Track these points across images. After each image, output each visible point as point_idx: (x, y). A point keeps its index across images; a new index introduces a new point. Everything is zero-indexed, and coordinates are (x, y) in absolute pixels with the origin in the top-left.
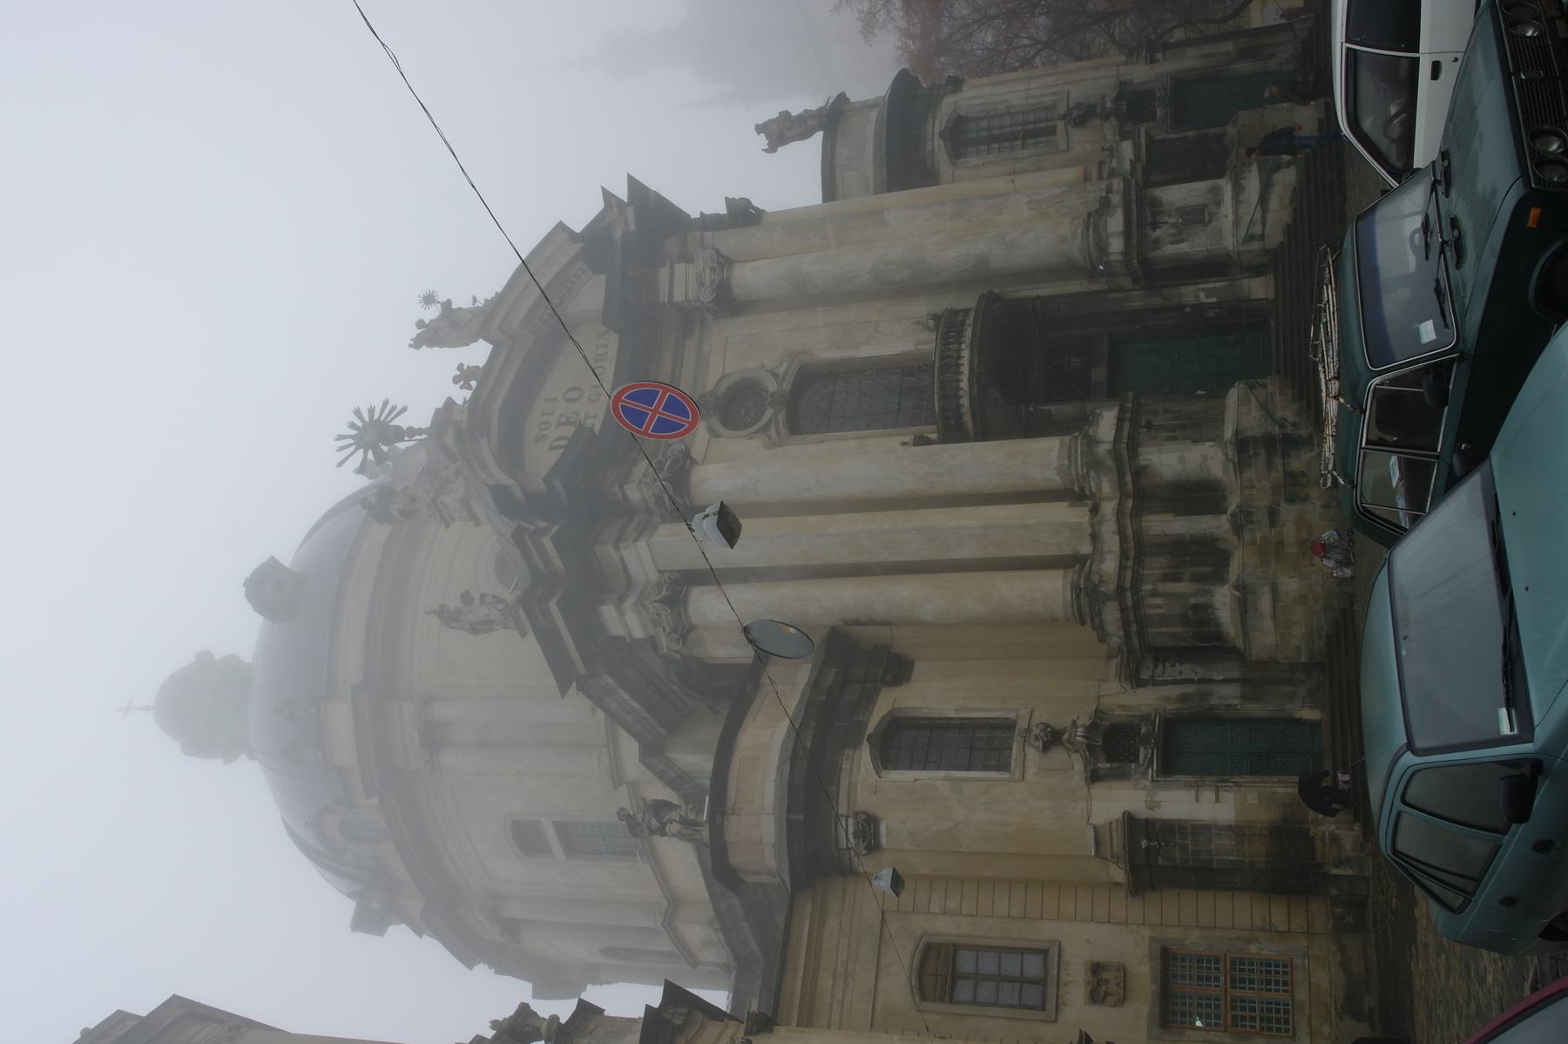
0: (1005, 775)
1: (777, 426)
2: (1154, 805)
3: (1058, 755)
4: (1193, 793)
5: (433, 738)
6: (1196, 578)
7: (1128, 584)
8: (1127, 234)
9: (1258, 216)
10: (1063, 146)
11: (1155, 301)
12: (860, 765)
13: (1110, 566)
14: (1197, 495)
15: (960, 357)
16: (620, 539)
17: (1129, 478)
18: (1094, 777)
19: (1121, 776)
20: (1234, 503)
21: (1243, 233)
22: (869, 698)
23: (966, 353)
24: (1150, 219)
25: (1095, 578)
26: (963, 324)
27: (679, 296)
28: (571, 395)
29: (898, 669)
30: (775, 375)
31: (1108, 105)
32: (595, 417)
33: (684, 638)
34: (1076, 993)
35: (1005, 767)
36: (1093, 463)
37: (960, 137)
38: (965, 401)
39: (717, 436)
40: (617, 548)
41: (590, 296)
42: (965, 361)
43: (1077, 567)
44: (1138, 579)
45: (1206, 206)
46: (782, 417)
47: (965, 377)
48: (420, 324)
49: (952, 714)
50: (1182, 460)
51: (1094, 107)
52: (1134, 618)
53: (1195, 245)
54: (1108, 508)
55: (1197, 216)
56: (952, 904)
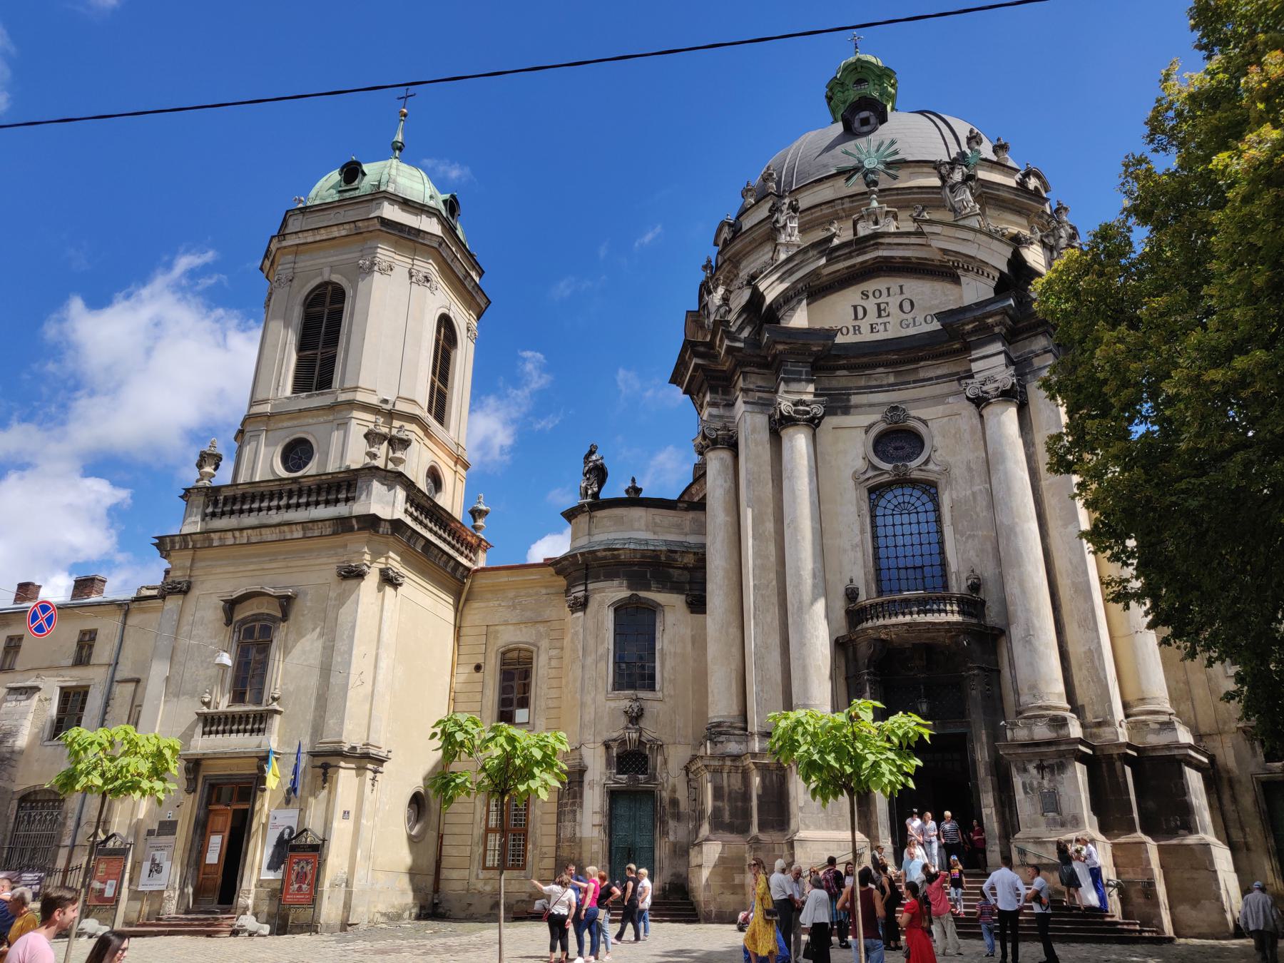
0: (610, 688)
3: (623, 721)
6: (717, 811)
11: (982, 771)
12: (616, 591)
13: (733, 747)
15: (904, 614)
18: (607, 746)
19: (609, 764)
23: (908, 618)
24: (1045, 764)
25: (722, 738)
27: (975, 367)
28: (907, 306)
30: (927, 462)
32: (886, 330)
39: (866, 432)
40: (742, 390)
41: (975, 290)
42: (901, 619)
43: (741, 725)
45: (1060, 814)
46: (885, 478)
49: (658, 646)
53: (1025, 806)
56: (554, 663)
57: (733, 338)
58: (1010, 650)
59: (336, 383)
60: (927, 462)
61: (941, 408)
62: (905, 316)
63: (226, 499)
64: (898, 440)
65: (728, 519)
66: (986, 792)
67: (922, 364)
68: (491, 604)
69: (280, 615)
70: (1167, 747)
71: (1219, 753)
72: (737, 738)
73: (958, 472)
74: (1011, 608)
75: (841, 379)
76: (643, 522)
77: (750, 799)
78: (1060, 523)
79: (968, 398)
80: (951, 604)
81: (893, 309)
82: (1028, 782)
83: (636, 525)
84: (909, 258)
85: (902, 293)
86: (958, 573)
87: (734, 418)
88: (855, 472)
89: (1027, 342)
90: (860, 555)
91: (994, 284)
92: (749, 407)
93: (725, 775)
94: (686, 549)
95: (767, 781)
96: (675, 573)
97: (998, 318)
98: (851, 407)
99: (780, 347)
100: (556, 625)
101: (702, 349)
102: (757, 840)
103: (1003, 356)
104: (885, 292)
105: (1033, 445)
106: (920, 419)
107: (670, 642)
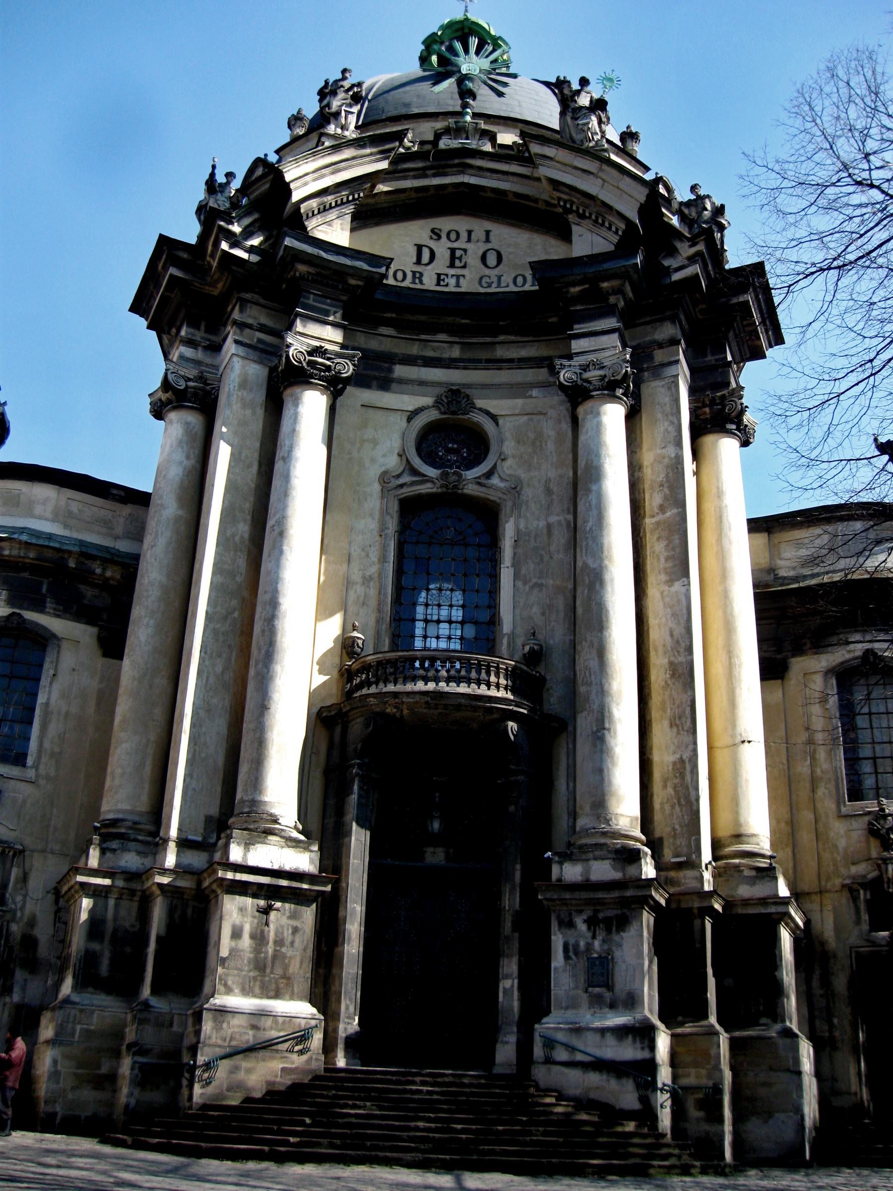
1: (413, 483)
6: (89, 960)
7: (80, 878)
8: (587, 886)
9: (579, 1057)
11: (508, 925)
16: (242, 326)
21: (560, 1036)
23: (431, 686)
26: (479, 683)
28: (492, 260)
30: (489, 475)
32: (458, 285)
39: (409, 420)
40: (235, 323)
42: (420, 686)
46: (426, 489)
48: (584, 82)
49: (41, 699)
53: (563, 977)
58: (572, 753)
60: (489, 475)
61: (519, 402)
62: (487, 272)
64: (453, 437)
65: (180, 512)
66: (510, 956)
67: (502, 338)
70: (763, 901)
71: (816, 917)
72: (140, 847)
74: (582, 689)
75: (384, 340)
76: (50, 508)
77: (146, 944)
78: (663, 577)
79: (561, 386)
80: (497, 675)
81: (473, 260)
82: (572, 941)
83: (38, 510)
84: (504, 193)
85: (488, 240)
86: (512, 636)
87: (217, 367)
88: (384, 474)
89: (648, 328)
90: (373, 592)
91: (615, 239)
92: (241, 351)
93: (111, 902)
94: (110, 557)
95: (176, 916)
96: (89, 592)
97: (615, 283)
98: (392, 380)
99: (302, 268)
101: (185, 256)
102: (146, 1005)
103: (615, 336)
104: (464, 236)
105: (640, 467)
106: (488, 413)
107: (64, 695)
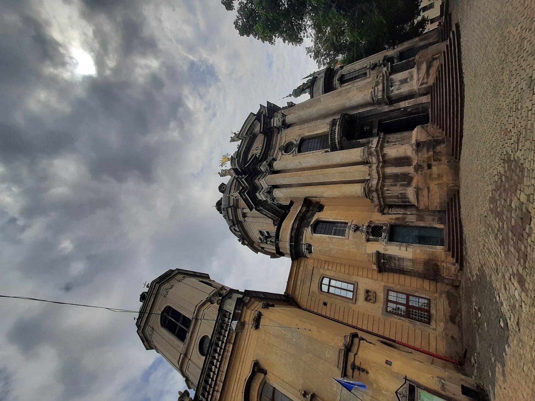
0: (344, 238)
2: (385, 250)
3: (358, 233)
4: (398, 247)
5: (244, 215)
9: (425, 77)
10: (368, 76)
11: (392, 108)
13: (374, 182)
14: (403, 161)
17: (381, 158)
18: (368, 240)
19: (377, 241)
20: (414, 163)
21: (420, 83)
22: (313, 215)
24: (390, 85)
25: (370, 185)
29: (321, 208)
31: (381, 62)
33: (273, 200)
34: (361, 296)
35: (343, 235)
36: (370, 154)
37: (343, 80)
38: (336, 141)
44: (383, 186)
45: (408, 78)
46: (297, 150)
47: (337, 135)
50: (398, 151)
51: (377, 64)
52: (382, 196)
53: (405, 89)
54: (374, 167)
55: (404, 81)
57: (242, 178)
59: (191, 318)
63: (203, 395)
66: (400, 105)
68: (300, 291)
69: (262, 376)
73: (300, 132)
100: (315, 265)
